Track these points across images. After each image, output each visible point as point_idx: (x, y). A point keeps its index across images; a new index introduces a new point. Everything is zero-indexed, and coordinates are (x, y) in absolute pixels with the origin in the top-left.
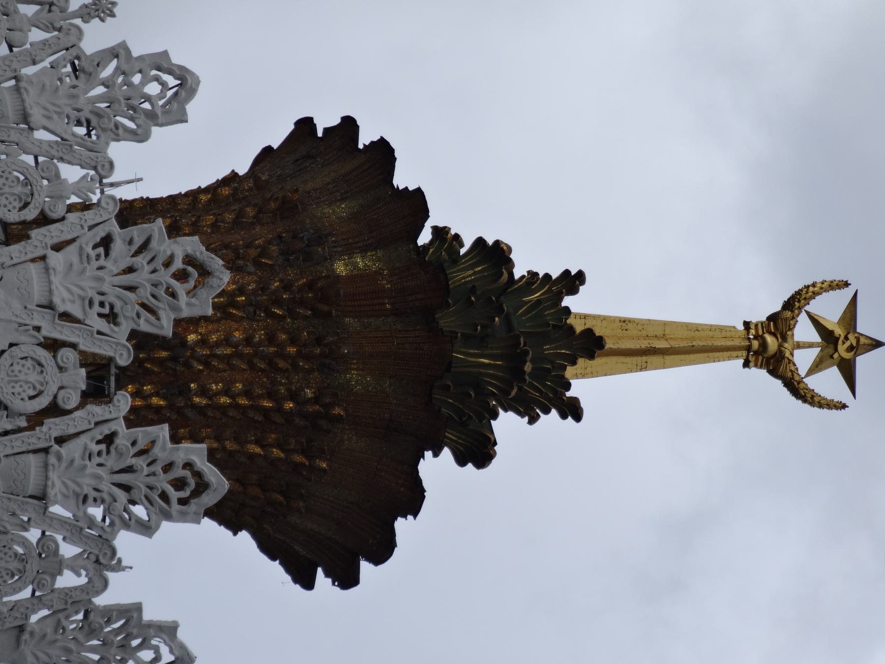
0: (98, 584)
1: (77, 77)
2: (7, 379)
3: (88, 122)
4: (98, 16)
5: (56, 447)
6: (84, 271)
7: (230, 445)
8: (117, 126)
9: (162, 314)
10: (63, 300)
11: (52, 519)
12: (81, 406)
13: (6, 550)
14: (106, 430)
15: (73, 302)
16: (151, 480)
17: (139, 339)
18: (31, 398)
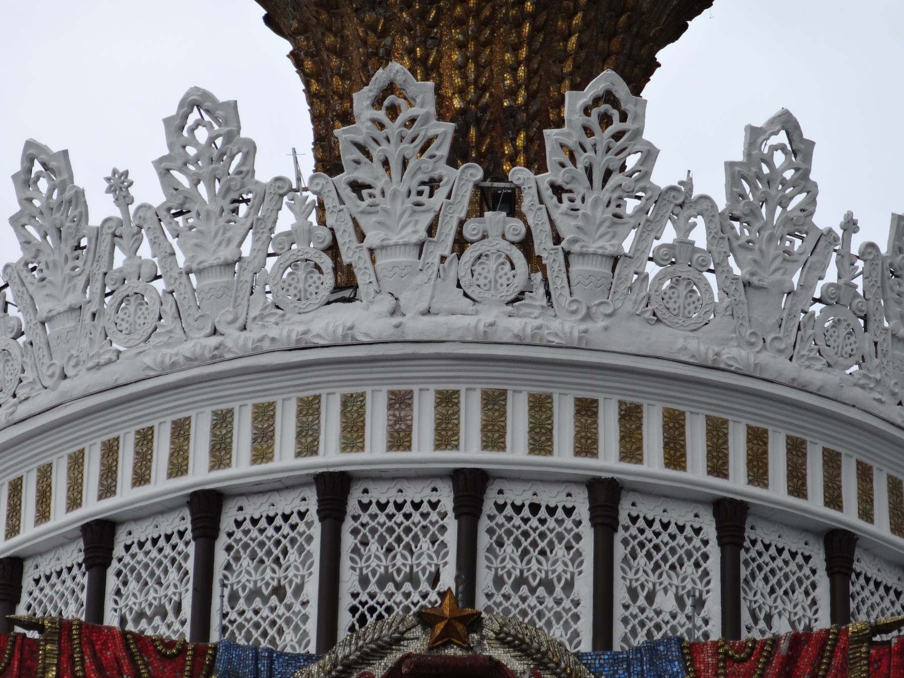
0: (705, 205)
1: (189, 212)
2: (493, 292)
3: (235, 201)
4: (127, 188)
5: (563, 244)
6: (385, 210)
7: (568, 67)
8: (239, 173)
9: (431, 133)
10: (415, 232)
11: (636, 250)
12: (522, 217)
13: (666, 297)
14: (548, 193)
15: (417, 222)
16: (601, 148)
17: (458, 156)
18: (513, 268)
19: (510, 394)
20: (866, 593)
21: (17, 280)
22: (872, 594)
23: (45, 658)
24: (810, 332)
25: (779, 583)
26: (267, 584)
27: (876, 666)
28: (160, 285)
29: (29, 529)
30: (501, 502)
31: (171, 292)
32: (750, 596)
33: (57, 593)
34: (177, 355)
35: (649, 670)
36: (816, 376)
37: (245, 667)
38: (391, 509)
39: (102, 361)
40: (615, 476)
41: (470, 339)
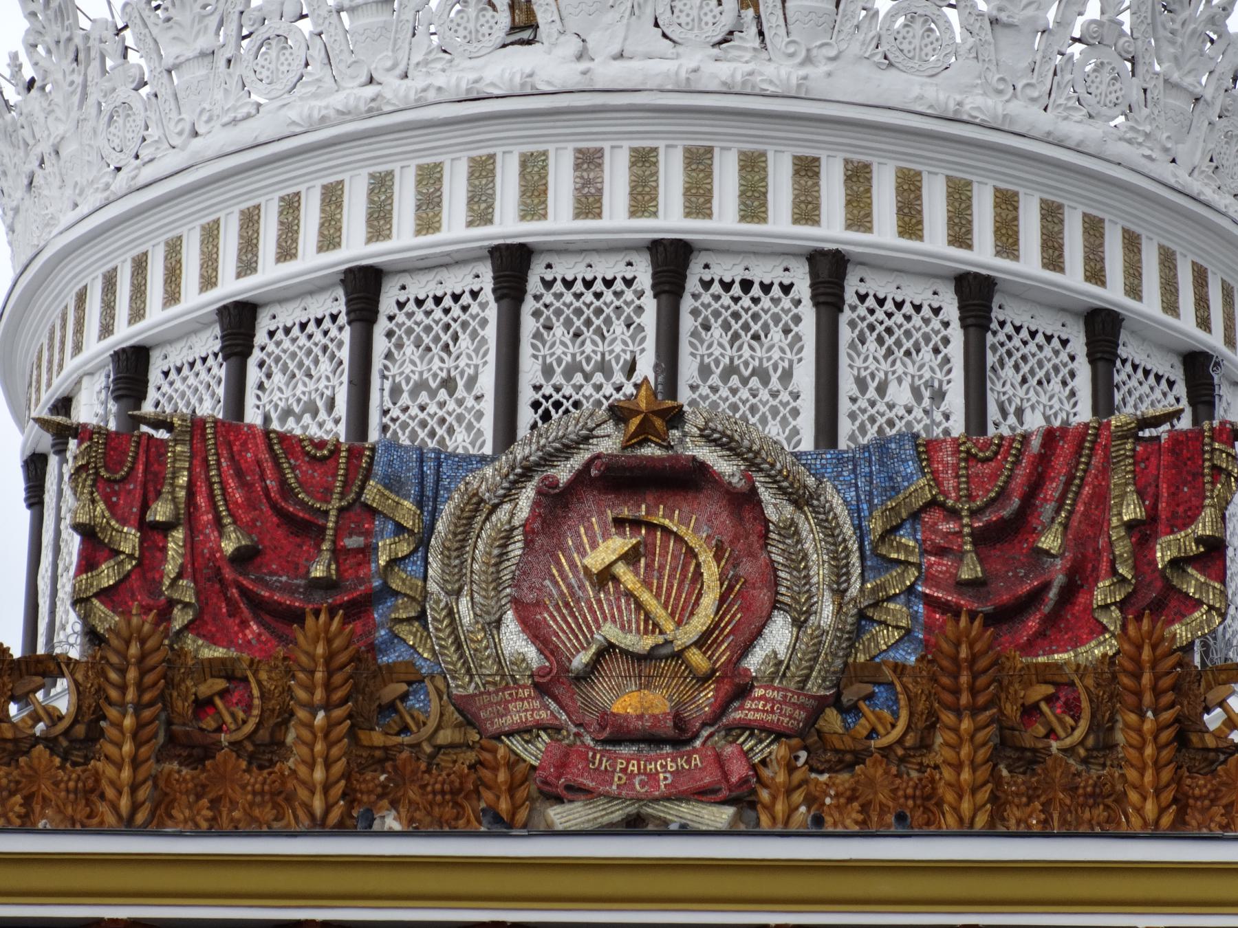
2: (696, 31)
13: (900, 37)
19: (716, 152)
20: (1133, 383)
21: (138, 21)
22: (1141, 383)
23: (175, 460)
24: (1068, 77)
25: (1032, 372)
26: (435, 376)
27: (1143, 465)
28: (306, 26)
29: (156, 313)
30: (707, 278)
31: (320, 34)
32: (999, 387)
33: (189, 387)
34: (327, 107)
35: (880, 472)
36: (1075, 129)
37: (409, 470)
38: (579, 287)
39: (239, 116)
40: (840, 247)
41: (670, 87)
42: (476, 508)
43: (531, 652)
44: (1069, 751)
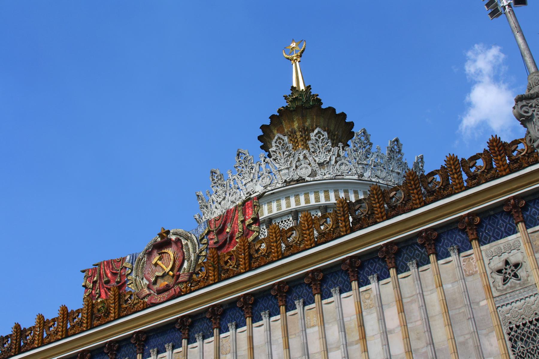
42: (140, 260)
43: (148, 283)
44: (234, 267)
